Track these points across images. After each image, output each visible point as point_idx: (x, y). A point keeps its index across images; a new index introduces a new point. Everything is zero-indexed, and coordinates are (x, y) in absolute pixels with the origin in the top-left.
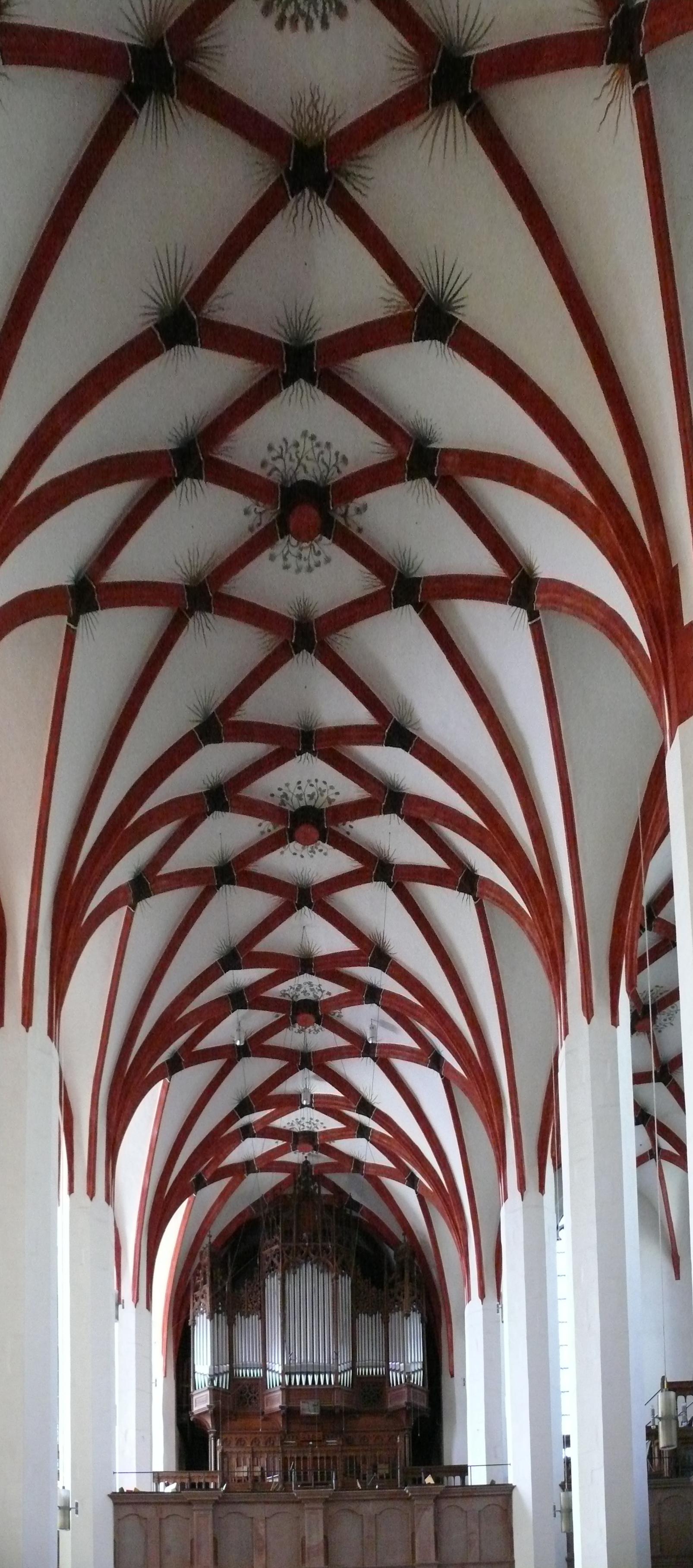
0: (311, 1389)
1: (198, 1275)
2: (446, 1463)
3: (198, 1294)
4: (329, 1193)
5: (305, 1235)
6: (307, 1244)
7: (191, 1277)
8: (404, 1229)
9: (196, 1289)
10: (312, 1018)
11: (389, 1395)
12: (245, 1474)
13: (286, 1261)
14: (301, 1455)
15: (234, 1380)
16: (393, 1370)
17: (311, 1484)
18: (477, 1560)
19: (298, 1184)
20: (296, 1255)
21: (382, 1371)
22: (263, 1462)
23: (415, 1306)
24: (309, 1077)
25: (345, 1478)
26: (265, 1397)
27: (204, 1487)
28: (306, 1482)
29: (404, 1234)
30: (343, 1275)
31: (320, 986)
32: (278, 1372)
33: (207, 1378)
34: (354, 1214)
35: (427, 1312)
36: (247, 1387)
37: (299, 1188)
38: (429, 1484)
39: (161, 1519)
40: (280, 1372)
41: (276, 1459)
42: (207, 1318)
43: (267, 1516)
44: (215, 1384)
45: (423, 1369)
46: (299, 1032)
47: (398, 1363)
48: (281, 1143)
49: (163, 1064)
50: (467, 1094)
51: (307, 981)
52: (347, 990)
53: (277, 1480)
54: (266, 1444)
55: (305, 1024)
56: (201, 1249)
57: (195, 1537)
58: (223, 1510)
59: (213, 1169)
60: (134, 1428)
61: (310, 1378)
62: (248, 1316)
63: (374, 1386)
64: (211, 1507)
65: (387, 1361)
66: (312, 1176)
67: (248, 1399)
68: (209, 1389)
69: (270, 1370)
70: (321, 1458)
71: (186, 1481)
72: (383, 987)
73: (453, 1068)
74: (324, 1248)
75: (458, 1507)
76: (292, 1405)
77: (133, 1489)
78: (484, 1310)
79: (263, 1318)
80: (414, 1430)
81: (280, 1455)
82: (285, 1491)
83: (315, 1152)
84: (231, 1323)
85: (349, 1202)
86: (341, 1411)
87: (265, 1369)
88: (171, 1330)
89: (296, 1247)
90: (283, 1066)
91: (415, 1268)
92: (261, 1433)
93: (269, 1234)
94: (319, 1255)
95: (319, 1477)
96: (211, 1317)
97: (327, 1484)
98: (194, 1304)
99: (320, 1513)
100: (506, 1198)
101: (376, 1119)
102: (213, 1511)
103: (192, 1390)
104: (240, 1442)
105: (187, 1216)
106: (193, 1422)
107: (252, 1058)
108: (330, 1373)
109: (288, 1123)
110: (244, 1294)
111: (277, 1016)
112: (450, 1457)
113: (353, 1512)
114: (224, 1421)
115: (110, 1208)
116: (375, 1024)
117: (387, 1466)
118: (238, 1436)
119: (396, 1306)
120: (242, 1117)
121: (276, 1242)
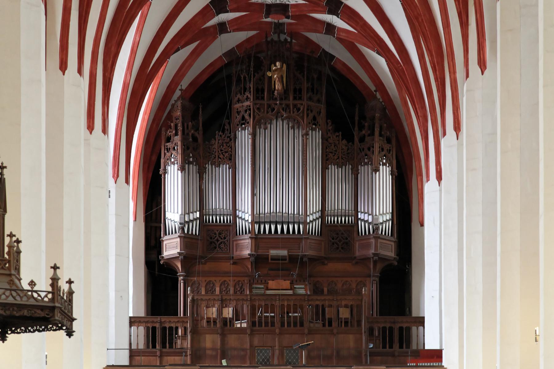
6: (278, 102)
13: (257, 117)
20: (268, 112)
26: (235, 243)
30: (312, 129)
32: (248, 220)
36: (217, 233)
40: (250, 221)
41: (245, 306)
42: (178, 170)
44: (186, 232)
45: (392, 220)
47: (366, 215)
65: (357, 212)
68: (179, 236)
69: (239, 218)
74: (295, 106)
76: (261, 252)
87: (235, 216)
89: (267, 104)
94: (290, 112)
96: (182, 169)
103: (162, 236)
121: (247, 99)
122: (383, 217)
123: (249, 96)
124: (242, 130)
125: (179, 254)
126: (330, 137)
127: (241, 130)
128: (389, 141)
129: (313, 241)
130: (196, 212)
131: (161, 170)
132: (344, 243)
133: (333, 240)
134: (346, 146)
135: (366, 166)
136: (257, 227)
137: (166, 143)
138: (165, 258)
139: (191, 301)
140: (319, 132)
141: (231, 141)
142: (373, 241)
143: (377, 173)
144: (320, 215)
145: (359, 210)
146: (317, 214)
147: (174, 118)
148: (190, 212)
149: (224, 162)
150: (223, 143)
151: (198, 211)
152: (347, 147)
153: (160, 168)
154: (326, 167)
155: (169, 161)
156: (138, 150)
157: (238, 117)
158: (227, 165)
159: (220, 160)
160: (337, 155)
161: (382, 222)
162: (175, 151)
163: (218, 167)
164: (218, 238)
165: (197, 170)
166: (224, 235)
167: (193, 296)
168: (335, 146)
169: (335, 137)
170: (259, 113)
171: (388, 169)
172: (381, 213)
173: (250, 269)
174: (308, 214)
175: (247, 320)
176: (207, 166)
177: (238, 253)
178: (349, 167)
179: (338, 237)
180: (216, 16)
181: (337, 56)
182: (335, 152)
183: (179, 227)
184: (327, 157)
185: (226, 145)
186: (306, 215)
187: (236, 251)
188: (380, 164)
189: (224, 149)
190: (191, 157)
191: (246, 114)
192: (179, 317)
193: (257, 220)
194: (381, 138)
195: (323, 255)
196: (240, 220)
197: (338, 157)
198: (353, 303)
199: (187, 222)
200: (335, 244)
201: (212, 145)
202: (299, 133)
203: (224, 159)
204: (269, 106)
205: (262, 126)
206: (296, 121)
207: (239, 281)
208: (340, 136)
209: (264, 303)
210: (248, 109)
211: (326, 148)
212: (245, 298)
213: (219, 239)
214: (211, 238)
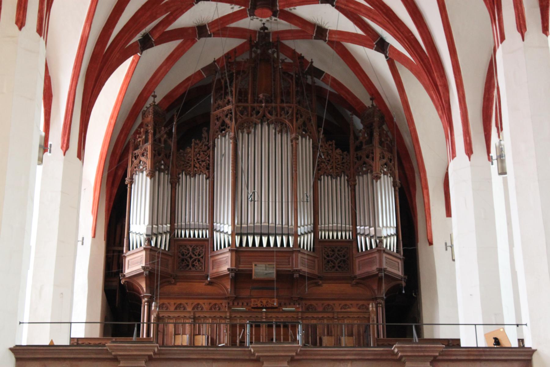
1: (140, 133)
3: (137, 152)
5: (261, 96)
6: (263, 105)
8: (371, 94)
9: (136, 147)
11: (357, 261)
13: (240, 120)
15: (174, 241)
20: (252, 115)
21: (348, 235)
26: (211, 260)
29: (371, 99)
32: (227, 233)
33: (143, 238)
36: (190, 249)
37: (255, 52)
40: (230, 232)
42: (147, 175)
44: (153, 244)
45: (397, 234)
47: (367, 228)
61: (265, 239)
62: (194, 176)
63: (339, 251)
65: (355, 224)
67: (191, 261)
68: (145, 249)
69: (217, 231)
76: (242, 267)
79: (211, 178)
84: (174, 183)
87: (212, 230)
89: (252, 107)
96: (152, 175)
98: (132, 162)
103: (124, 251)
105: (130, 74)
106: (124, 284)
108: (288, 235)
110: (191, 152)
119: (364, 169)
121: (228, 102)
122: (387, 230)
123: (230, 98)
127: (221, 137)
128: (391, 151)
129: (306, 257)
130: (166, 224)
132: (341, 261)
133: (328, 258)
135: (365, 176)
136: (238, 239)
137: (134, 151)
139: (155, 319)
140: (309, 139)
141: (209, 150)
142: (377, 255)
143: (379, 181)
144: (312, 229)
145: (358, 224)
146: (309, 226)
147: (144, 124)
148: (159, 223)
149: (201, 171)
150: (199, 152)
151: (169, 224)
152: (342, 157)
153: (126, 177)
154: (318, 177)
155: (137, 169)
157: (217, 123)
159: (196, 169)
160: (331, 164)
162: (145, 157)
163: (194, 177)
164: (191, 255)
165: (169, 180)
166: (198, 251)
168: (328, 155)
169: (327, 145)
170: (241, 116)
171: (390, 180)
172: (385, 225)
173: (229, 290)
174: (299, 225)
176: (180, 176)
178: (344, 178)
179: (333, 255)
182: (328, 162)
183: (145, 239)
184: (319, 167)
185: (204, 154)
186: (296, 226)
187: (213, 269)
188: (381, 172)
189: (200, 158)
190: (162, 164)
191: (227, 119)
192: (141, 339)
193: (238, 232)
194: (380, 147)
195: (316, 273)
196: (218, 234)
197: (331, 167)
198: (357, 322)
199: (155, 234)
200: (331, 262)
201: (188, 153)
202: (286, 139)
203: (200, 168)
204: (253, 109)
205: (245, 130)
207: (215, 304)
208: (334, 145)
212: (223, 316)
213: (193, 256)
214: (183, 255)
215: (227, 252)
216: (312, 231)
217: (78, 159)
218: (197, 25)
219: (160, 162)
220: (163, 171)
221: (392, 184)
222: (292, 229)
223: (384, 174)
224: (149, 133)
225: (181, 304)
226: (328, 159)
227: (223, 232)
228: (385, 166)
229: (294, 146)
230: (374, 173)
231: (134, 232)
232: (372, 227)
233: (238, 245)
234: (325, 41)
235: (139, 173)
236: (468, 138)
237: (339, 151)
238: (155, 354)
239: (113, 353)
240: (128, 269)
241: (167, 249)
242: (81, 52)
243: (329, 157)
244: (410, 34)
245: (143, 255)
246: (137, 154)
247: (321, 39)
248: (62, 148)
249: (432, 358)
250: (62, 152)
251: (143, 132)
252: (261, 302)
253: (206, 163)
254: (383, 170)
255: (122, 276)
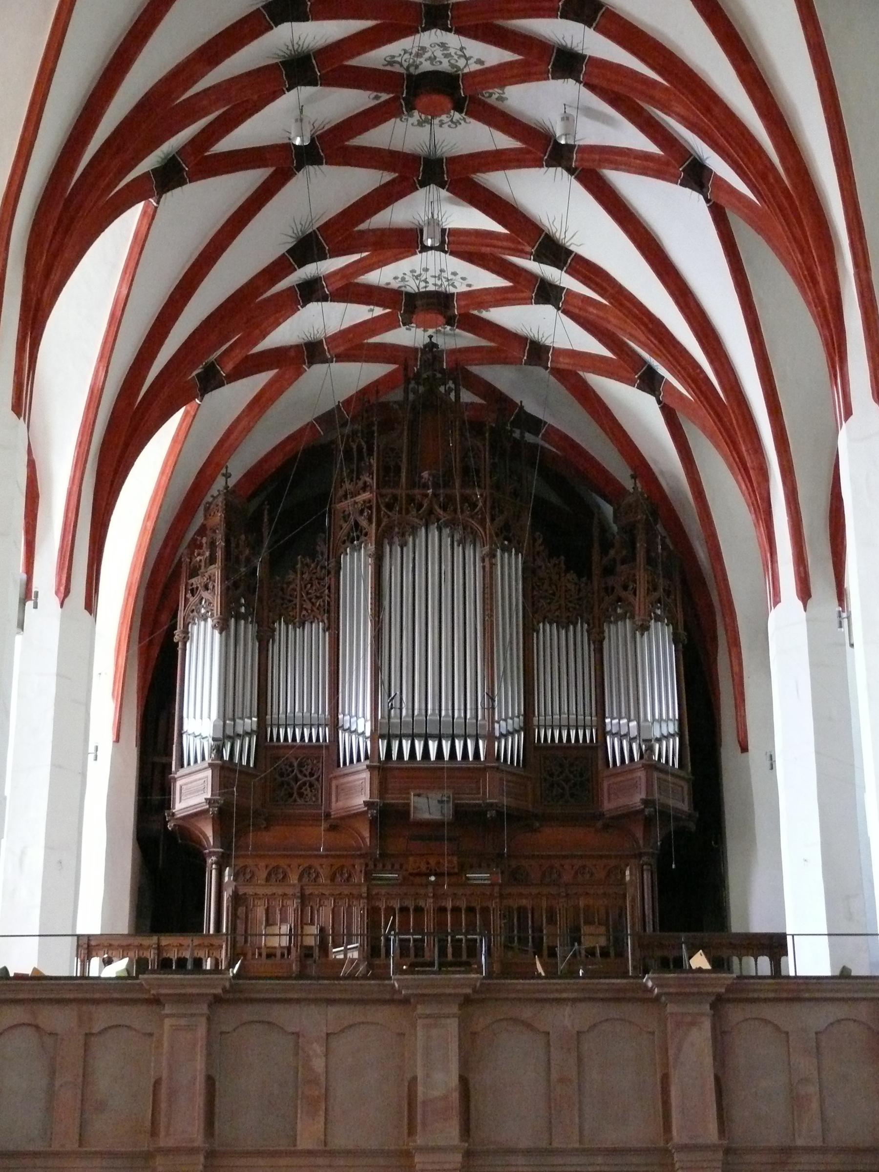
0: (435, 769)
2: (736, 926)
3: (195, 581)
4: (477, 400)
5: (425, 474)
6: (430, 491)
7: (183, 549)
8: (634, 468)
9: (194, 572)
10: (447, 102)
12: (285, 941)
13: (385, 521)
14: (410, 904)
16: (614, 735)
17: (432, 964)
18: (819, 1143)
19: (412, 385)
20: (408, 512)
21: (590, 734)
22: (325, 915)
23: (659, 612)
24: (439, 200)
25: (510, 954)
26: (334, 783)
27: (189, 967)
28: (420, 960)
29: (634, 477)
30: (503, 550)
31: (462, 49)
32: (363, 733)
33: (208, 744)
34: (530, 438)
35: (685, 622)
36: (296, 764)
38: (700, 970)
39: (88, 1035)
40: (368, 734)
42: (214, 627)
43: (329, 1032)
44: (226, 757)
45: (681, 734)
46: (420, 124)
48: (379, 311)
49: (146, 175)
50: (760, 230)
51: (438, 41)
52: (516, 57)
53: (356, 955)
54: (333, 879)
55: (433, 112)
56: (208, 499)
57: (165, 1075)
58: (229, 1017)
59: (238, 355)
60: (42, 843)
61: (433, 746)
62: (303, 624)
64: (204, 1009)
66: (442, 371)
68: (210, 765)
69: (345, 730)
70: (456, 910)
71: (151, 955)
72: (588, 53)
73: (729, 186)
74: (465, 499)
75: (766, 1022)
76: (391, 799)
77: (28, 971)
78: (808, 620)
79: (333, 628)
80: (663, 858)
81: (363, 902)
82: (374, 977)
83: (448, 328)
84: (264, 639)
85: (518, 415)
86: (500, 814)
87: (335, 726)
88: (135, 648)
90: (384, 181)
91: (659, 540)
92: (322, 856)
93: (352, 471)
94: (455, 511)
95: (450, 950)
96: (223, 626)
97: (468, 964)
98: (186, 600)
99: (453, 1025)
100: (848, 413)
101: (573, 272)
102: (208, 1019)
103: (173, 769)
104: (276, 875)
106: (173, 831)
107: (324, 167)
109: (396, 278)
110: (296, 580)
111: (377, 98)
112: (745, 916)
113: (529, 1026)
114: (242, 832)
115: (22, 424)
116: (571, 111)
117: (602, 929)
118: (273, 863)
120: (300, 266)
121: (365, 488)
123: (368, 479)
124: (353, 549)
125: (209, 803)
126: (540, 567)
127: (350, 552)
130: (250, 718)
131: (177, 632)
134: (576, 584)
136: (382, 745)
138: (178, 816)
140: (517, 555)
141: (330, 576)
143: (646, 634)
144: (522, 725)
145: (607, 715)
146: (516, 720)
148: (236, 716)
149: (314, 617)
150: (311, 579)
152: (577, 587)
153: (176, 629)
155: (195, 613)
156: (129, 594)
157: (345, 525)
158: (321, 624)
159: (304, 612)
160: (557, 601)
161: (658, 736)
162: (209, 591)
164: (296, 775)
166: (310, 767)
167: (236, 887)
170: (389, 513)
171: (668, 631)
172: (657, 717)
173: (368, 840)
174: (496, 718)
175: (360, 945)
176: (277, 625)
177: (341, 804)
178: (581, 628)
179: (561, 773)
180: (302, 307)
181: (550, 420)
183: (212, 746)
187: (337, 801)
190: (241, 605)
194: (650, 568)
199: (229, 737)
201: (289, 583)
202: (473, 555)
203: (312, 611)
204: (411, 499)
206: (469, 530)
208: (563, 566)
209: (400, 904)
210: (367, 504)
211: (533, 588)
212: (355, 892)
213: (299, 776)
215: (363, 770)
216: (521, 728)
217: (86, 613)
218: (306, 340)
219: (239, 599)
220: (245, 617)
221: (671, 637)
222: (483, 726)
223: (656, 621)
224: (216, 547)
225: (278, 867)
226: (551, 592)
227: (355, 731)
228: (659, 605)
229: (487, 569)
230: (637, 618)
231: (190, 732)
232: (633, 721)
233: (383, 757)
234: (546, 368)
235: (198, 620)
236: (802, 569)
237: (572, 576)
238: (225, 990)
239: (152, 992)
240: (180, 801)
241: (252, 765)
242: (91, 416)
243: (554, 587)
244: (699, 371)
245: (207, 777)
246: (195, 586)
247: (539, 365)
248: (57, 593)
249: (713, 998)
250: (56, 601)
251: (206, 543)
252: (428, 863)
253: (324, 601)
254: (654, 613)
255: (169, 815)
